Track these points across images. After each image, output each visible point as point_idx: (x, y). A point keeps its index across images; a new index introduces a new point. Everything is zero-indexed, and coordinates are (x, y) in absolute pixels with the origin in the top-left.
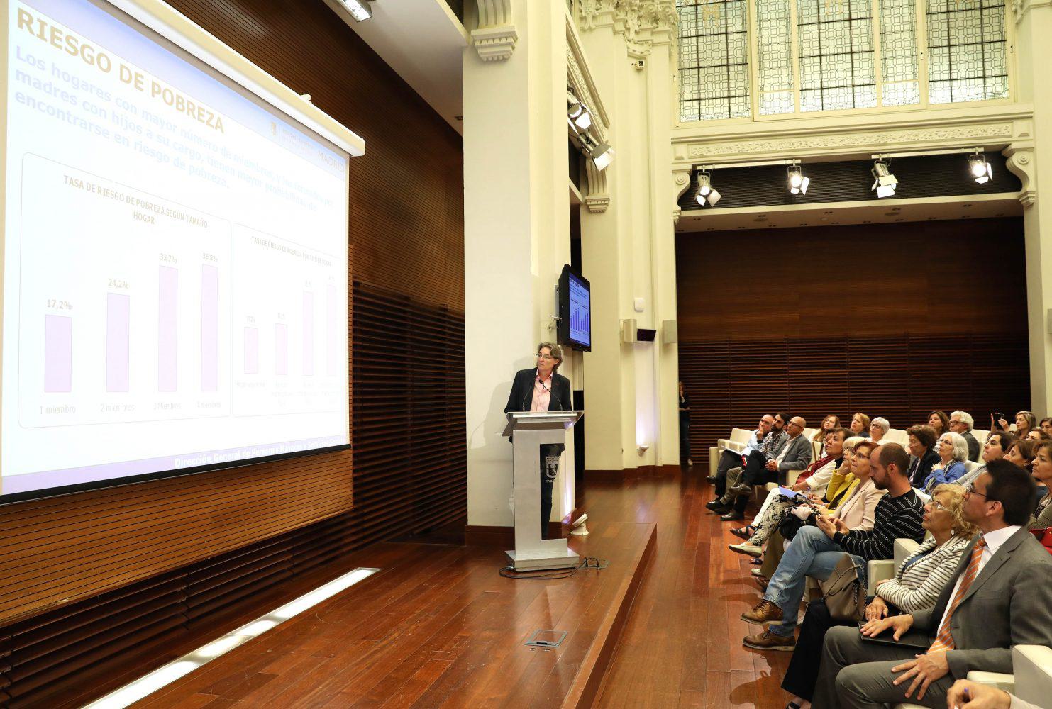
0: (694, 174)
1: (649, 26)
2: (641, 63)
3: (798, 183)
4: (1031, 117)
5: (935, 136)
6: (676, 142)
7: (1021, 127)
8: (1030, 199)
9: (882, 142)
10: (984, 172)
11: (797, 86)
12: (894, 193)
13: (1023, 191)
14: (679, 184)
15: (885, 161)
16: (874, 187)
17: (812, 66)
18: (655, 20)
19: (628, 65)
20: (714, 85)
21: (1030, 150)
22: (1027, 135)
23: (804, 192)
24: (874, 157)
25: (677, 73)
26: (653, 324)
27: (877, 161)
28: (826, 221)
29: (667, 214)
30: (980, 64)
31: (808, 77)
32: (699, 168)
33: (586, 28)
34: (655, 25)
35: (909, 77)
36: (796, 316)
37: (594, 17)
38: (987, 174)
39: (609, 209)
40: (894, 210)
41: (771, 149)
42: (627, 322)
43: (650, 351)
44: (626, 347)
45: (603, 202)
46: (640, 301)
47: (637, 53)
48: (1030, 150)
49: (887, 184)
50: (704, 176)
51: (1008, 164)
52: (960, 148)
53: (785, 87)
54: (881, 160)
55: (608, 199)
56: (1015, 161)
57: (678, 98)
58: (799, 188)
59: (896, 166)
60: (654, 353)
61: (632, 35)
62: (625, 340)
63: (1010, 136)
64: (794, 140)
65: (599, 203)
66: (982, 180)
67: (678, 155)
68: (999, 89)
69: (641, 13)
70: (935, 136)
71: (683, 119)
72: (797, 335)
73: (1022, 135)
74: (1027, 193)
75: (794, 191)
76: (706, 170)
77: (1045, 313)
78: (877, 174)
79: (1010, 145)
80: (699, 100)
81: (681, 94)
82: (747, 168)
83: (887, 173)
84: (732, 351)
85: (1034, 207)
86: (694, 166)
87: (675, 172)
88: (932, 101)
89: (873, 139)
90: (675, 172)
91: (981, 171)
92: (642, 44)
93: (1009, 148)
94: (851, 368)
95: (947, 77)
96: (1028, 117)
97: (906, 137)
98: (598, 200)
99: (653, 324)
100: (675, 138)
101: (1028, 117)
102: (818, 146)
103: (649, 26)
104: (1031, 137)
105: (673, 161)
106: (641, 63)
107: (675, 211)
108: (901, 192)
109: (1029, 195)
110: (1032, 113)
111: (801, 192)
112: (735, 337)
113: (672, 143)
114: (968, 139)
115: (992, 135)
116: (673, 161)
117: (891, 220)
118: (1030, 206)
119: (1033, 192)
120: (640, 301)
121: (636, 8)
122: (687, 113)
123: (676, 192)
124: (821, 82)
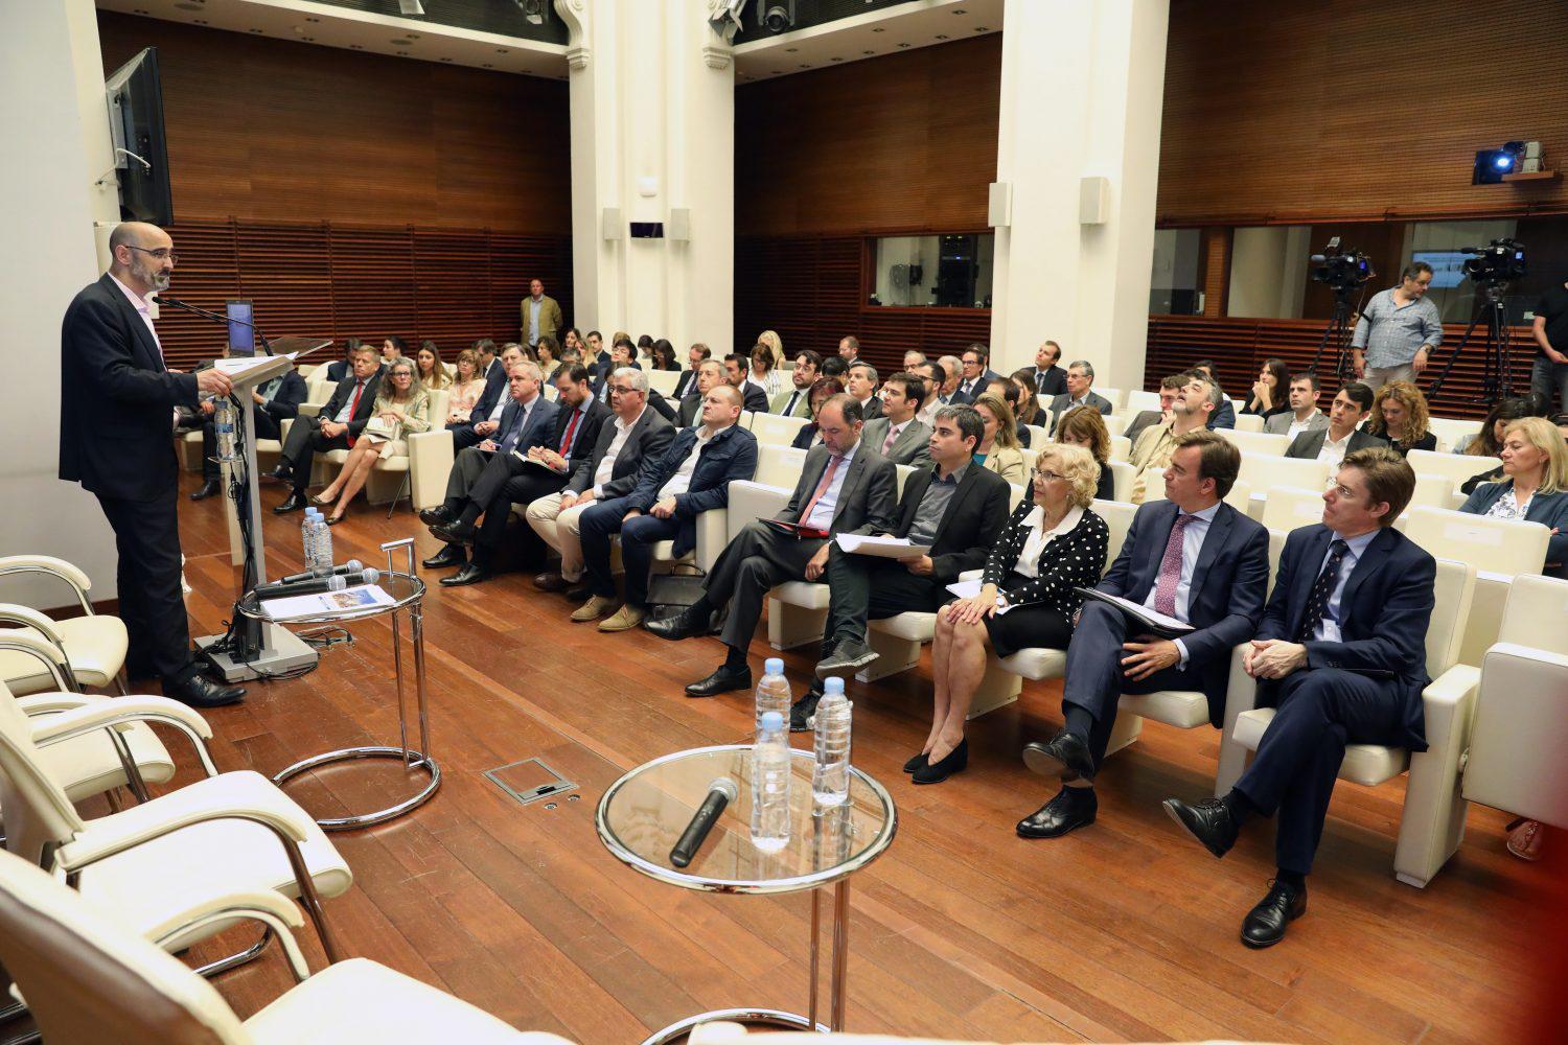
8: (583, 59)
13: (573, 45)
36: (245, 185)
72: (247, 217)
77: (599, 213)
85: (587, 69)
94: (335, 274)
109: (582, 54)
118: (581, 68)
119: (587, 50)
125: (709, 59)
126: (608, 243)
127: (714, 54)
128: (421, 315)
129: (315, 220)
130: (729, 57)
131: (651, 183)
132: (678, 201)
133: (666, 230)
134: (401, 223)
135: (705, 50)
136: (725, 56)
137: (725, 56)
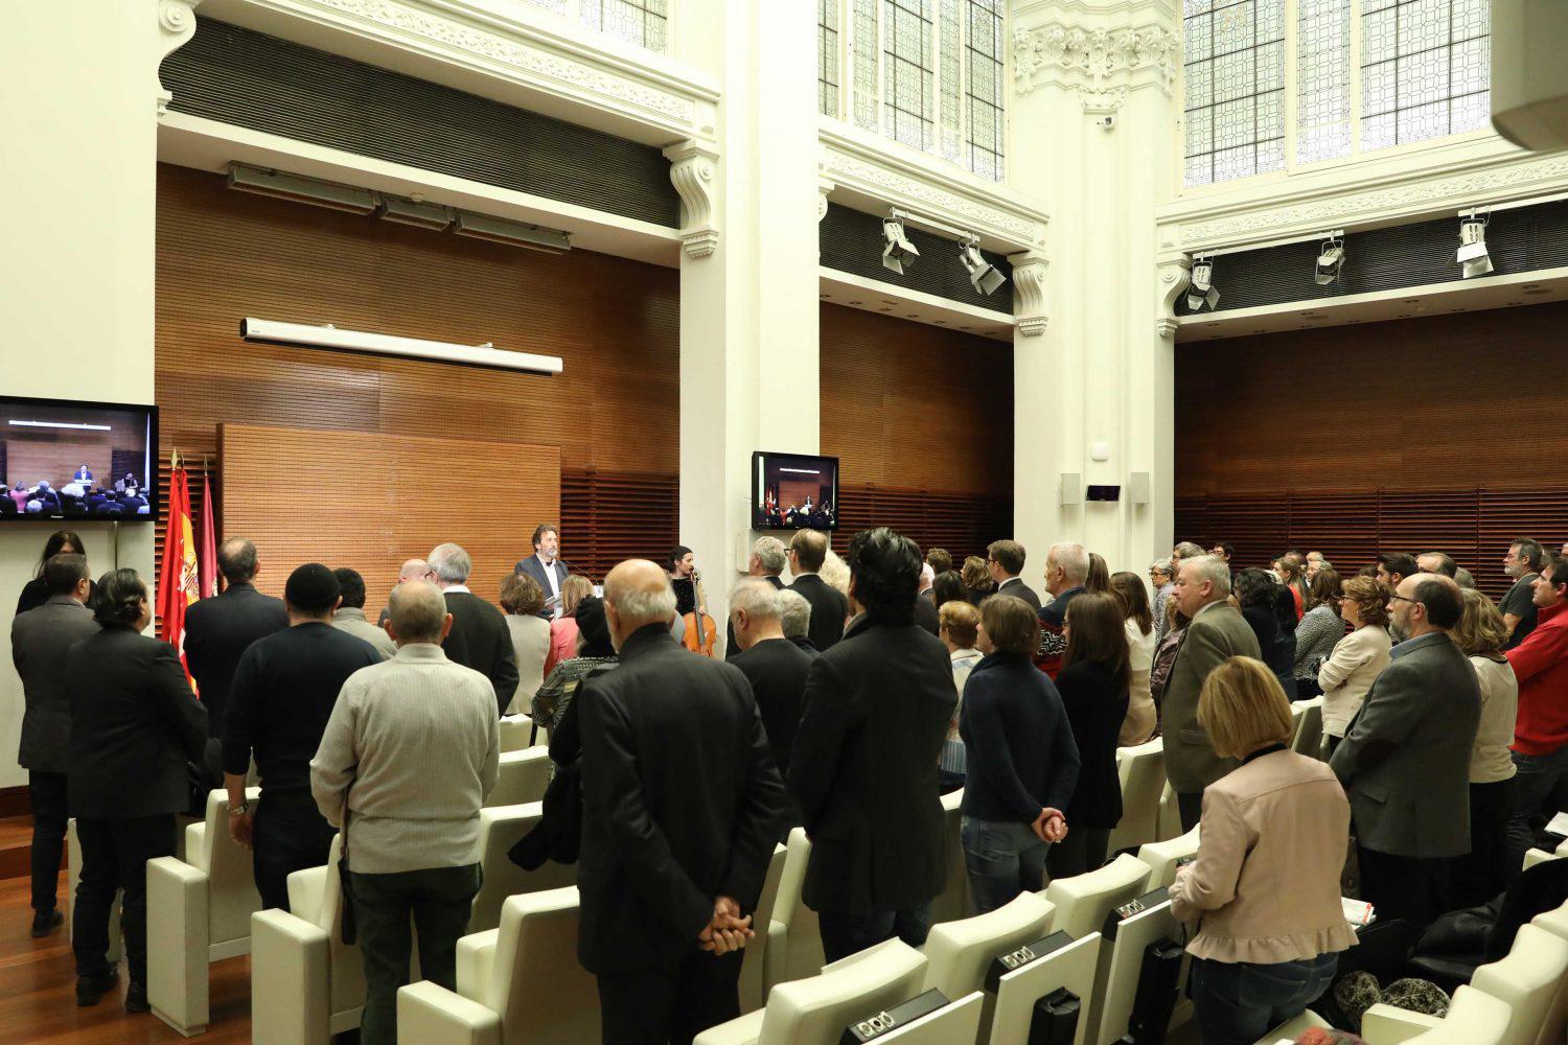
0: (1191, 263)
1: (1125, 64)
2: (1109, 120)
9: (1475, 189)
11: (1357, 112)
17: (1383, 76)
18: (1135, 53)
19: (1094, 124)
20: (1235, 125)
24: (1461, 214)
25: (1183, 117)
27: (1467, 220)
32: (1195, 256)
33: (1022, 91)
34: (1135, 61)
36: (1396, 457)
37: (1032, 75)
39: (1048, 331)
41: (1297, 219)
44: (1066, 511)
45: (1038, 323)
47: (1105, 107)
54: (1473, 217)
61: (1098, 84)
65: (1034, 323)
67: (1166, 241)
69: (1112, 49)
71: (1190, 183)
72: (1393, 487)
76: (1205, 259)
87: (1160, 265)
89: (1459, 187)
90: (1160, 265)
92: (1113, 93)
97: (1519, 176)
98: (1031, 320)
100: (1162, 218)
102: (1369, 207)
103: (1125, 64)
105: (1160, 250)
106: (1109, 120)
116: (1160, 250)
120: (1099, 447)
121: (1101, 45)
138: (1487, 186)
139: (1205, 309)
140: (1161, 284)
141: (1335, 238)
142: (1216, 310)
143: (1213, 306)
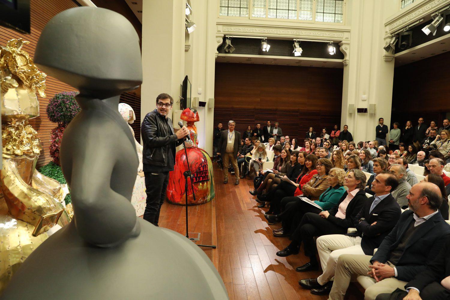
0: (225, 38)
3: (266, 47)
4: (350, 32)
5: (317, 34)
6: (218, 24)
7: (346, 35)
8: (347, 63)
9: (298, 34)
10: (333, 51)
11: (268, 7)
12: (300, 55)
13: (344, 59)
14: (218, 42)
15: (298, 42)
16: (293, 52)
21: (348, 44)
22: (348, 38)
23: (268, 51)
24: (294, 40)
26: (205, 100)
28: (273, 63)
29: (213, 54)
30: (334, 8)
31: (272, 4)
32: (227, 36)
35: (309, 9)
36: (259, 99)
38: (333, 52)
40: (299, 61)
41: (256, 32)
42: (195, 98)
43: (203, 110)
45: (188, 47)
46: (200, 90)
48: (348, 44)
49: (298, 51)
50: (229, 40)
51: (341, 48)
52: (325, 40)
53: (263, 7)
55: (190, 46)
56: (343, 48)
57: (220, 6)
58: (266, 49)
59: (303, 44)
60: (205, 112)
62: (194, 106)
63: (342, 38)
64: (265, 29)
66: (332, 54)
68: (339, 19)
70: (317, 34)
71: (221, 15)
72: (258, 107)
73: (346, 38)
74: (346, 60)
75: (264, 50)
76: (230, 37)
77: (348, 105)
78: (295, 47)
79: (342, 41)
80: (228, 7)
81: (221, 4)
82: (311, 42)
83: (299, 47)
84: (234, 112)
85: (348, 65)
86: (225, 35)
87: (217, 37)
88: (316, 20)
89: (295, 33)
90: (217, 37)
91: (332, 50)
93: (342, 42)
95: (322, 11)
96: (349, 31)
99: (205, 100)
100: (218, 23)
101: (349, 31)
104: (349, 39)
107: (216, 54)
108: (303, 55)
109: (346, 61)
110: (350, 30)
111: (266, 50)
112: (235, 106)
113: (217, 24)
114: (328, 37)
115: (336, 37)
117: (297, 65)
118: (346, 65)
119: (348, 60)
120: (200, 90)
122: (223, 12)
123: (218, 45)
124: (277, 6)
125: (385, 59)
126: (351, 114)
127: (387, 57)
128: (299, 133)
129: (275, 108)
130: (392, 58)
131: (365, 97)
132: (373, 101)
133: (368, 110)
134: (297, 108)
135: (384, 57)
136: (391, 58)
137: (391, 58)
138: (300, 34)
139: (229, 53)
140: (217, 42)
141: (265, 39)
142: (233, 53)
143: (231, 52)
